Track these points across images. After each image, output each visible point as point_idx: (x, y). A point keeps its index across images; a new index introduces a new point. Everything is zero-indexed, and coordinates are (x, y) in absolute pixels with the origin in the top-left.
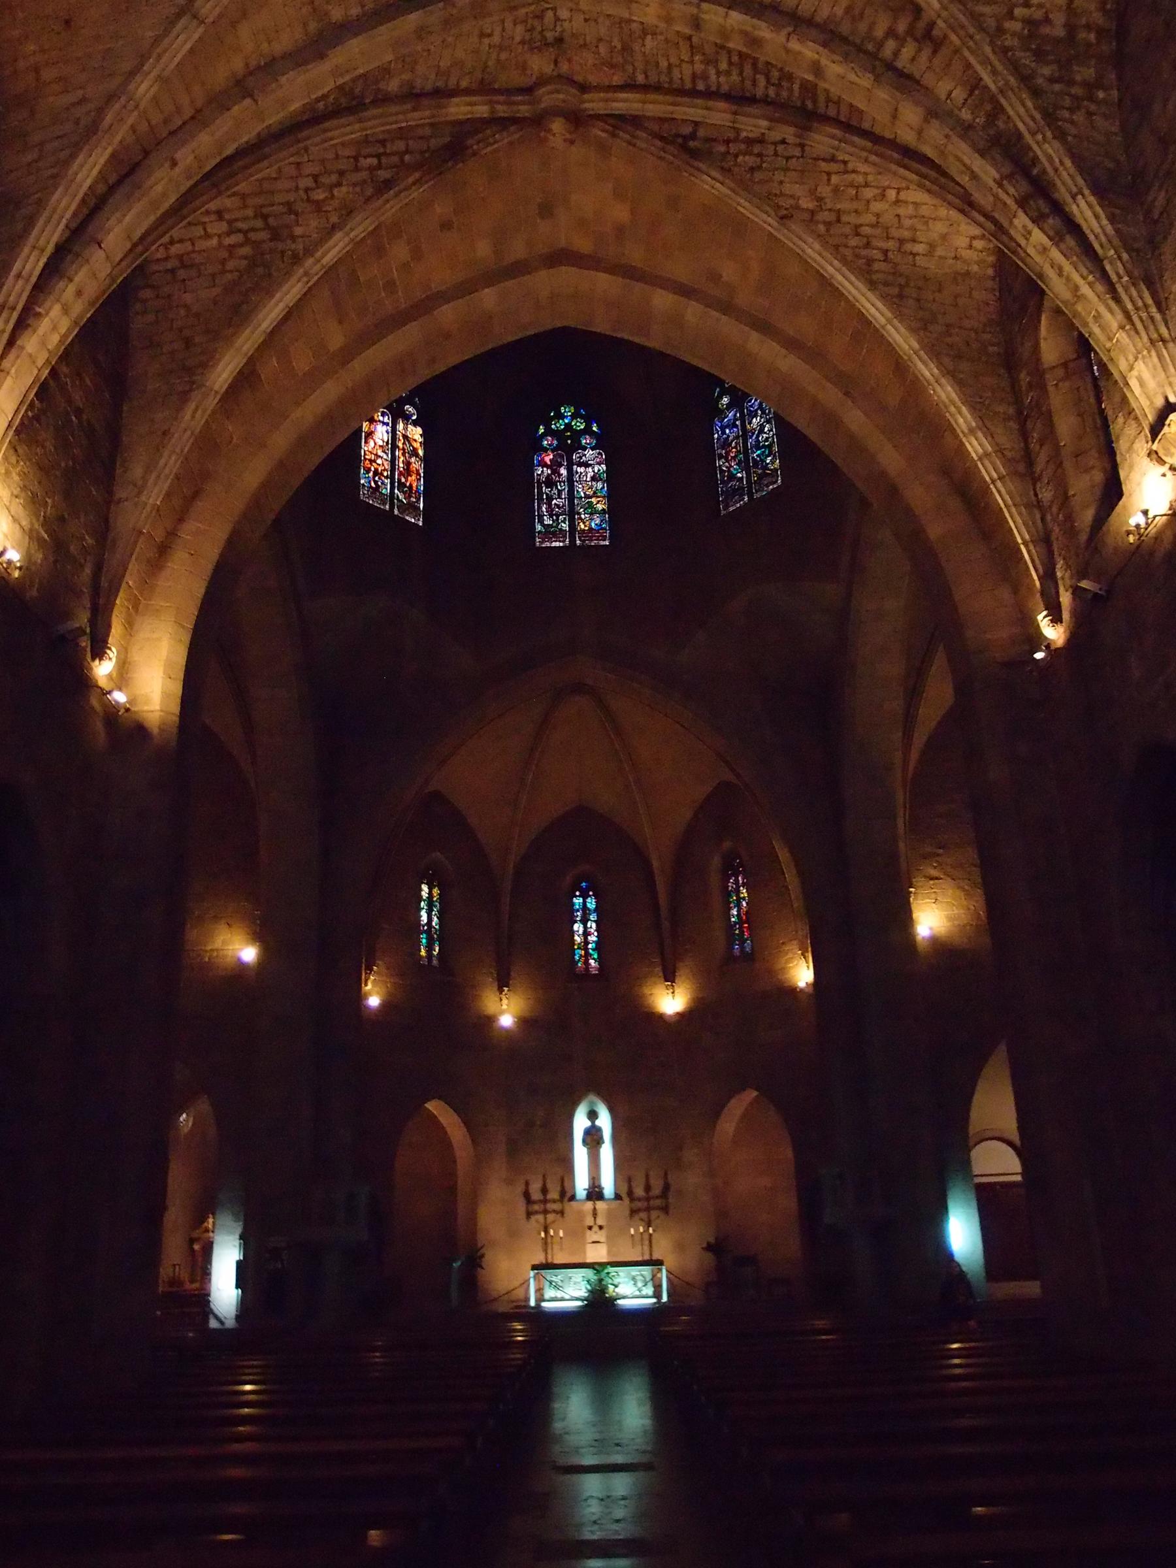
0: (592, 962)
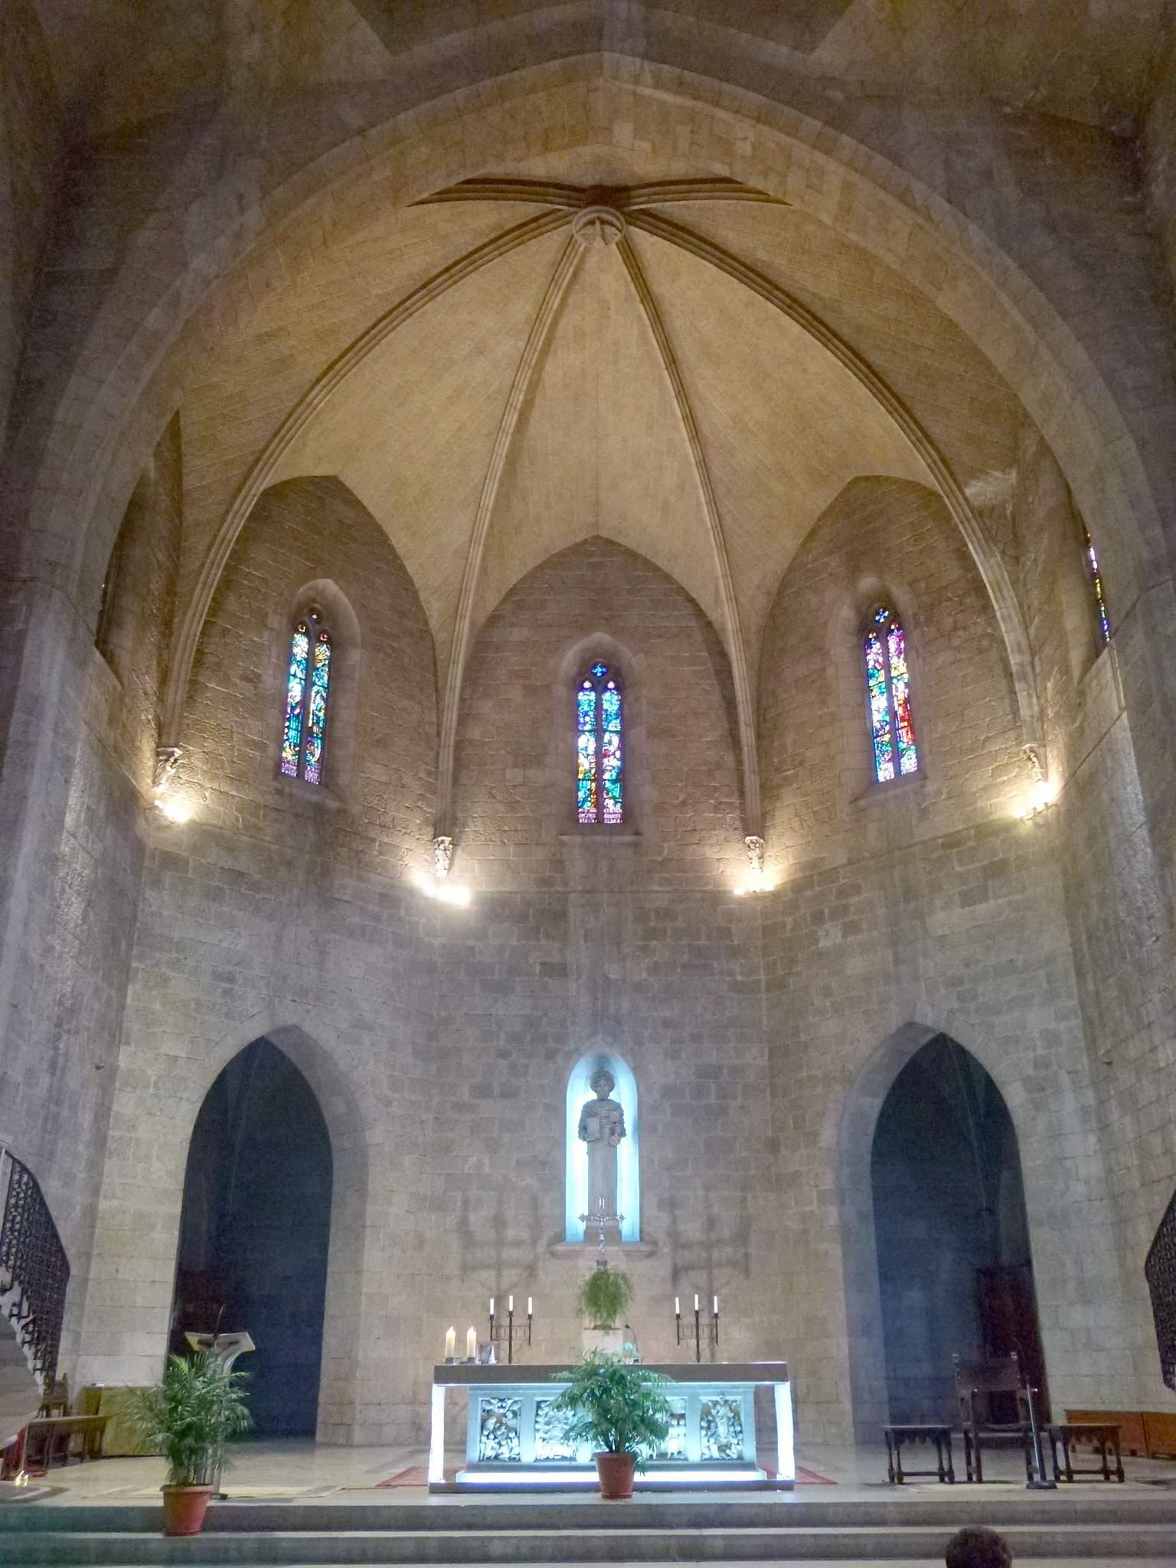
0: (609, 803)
